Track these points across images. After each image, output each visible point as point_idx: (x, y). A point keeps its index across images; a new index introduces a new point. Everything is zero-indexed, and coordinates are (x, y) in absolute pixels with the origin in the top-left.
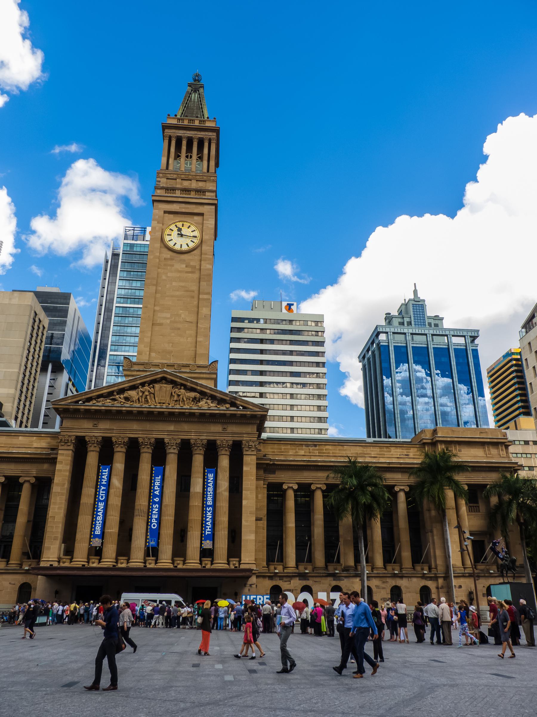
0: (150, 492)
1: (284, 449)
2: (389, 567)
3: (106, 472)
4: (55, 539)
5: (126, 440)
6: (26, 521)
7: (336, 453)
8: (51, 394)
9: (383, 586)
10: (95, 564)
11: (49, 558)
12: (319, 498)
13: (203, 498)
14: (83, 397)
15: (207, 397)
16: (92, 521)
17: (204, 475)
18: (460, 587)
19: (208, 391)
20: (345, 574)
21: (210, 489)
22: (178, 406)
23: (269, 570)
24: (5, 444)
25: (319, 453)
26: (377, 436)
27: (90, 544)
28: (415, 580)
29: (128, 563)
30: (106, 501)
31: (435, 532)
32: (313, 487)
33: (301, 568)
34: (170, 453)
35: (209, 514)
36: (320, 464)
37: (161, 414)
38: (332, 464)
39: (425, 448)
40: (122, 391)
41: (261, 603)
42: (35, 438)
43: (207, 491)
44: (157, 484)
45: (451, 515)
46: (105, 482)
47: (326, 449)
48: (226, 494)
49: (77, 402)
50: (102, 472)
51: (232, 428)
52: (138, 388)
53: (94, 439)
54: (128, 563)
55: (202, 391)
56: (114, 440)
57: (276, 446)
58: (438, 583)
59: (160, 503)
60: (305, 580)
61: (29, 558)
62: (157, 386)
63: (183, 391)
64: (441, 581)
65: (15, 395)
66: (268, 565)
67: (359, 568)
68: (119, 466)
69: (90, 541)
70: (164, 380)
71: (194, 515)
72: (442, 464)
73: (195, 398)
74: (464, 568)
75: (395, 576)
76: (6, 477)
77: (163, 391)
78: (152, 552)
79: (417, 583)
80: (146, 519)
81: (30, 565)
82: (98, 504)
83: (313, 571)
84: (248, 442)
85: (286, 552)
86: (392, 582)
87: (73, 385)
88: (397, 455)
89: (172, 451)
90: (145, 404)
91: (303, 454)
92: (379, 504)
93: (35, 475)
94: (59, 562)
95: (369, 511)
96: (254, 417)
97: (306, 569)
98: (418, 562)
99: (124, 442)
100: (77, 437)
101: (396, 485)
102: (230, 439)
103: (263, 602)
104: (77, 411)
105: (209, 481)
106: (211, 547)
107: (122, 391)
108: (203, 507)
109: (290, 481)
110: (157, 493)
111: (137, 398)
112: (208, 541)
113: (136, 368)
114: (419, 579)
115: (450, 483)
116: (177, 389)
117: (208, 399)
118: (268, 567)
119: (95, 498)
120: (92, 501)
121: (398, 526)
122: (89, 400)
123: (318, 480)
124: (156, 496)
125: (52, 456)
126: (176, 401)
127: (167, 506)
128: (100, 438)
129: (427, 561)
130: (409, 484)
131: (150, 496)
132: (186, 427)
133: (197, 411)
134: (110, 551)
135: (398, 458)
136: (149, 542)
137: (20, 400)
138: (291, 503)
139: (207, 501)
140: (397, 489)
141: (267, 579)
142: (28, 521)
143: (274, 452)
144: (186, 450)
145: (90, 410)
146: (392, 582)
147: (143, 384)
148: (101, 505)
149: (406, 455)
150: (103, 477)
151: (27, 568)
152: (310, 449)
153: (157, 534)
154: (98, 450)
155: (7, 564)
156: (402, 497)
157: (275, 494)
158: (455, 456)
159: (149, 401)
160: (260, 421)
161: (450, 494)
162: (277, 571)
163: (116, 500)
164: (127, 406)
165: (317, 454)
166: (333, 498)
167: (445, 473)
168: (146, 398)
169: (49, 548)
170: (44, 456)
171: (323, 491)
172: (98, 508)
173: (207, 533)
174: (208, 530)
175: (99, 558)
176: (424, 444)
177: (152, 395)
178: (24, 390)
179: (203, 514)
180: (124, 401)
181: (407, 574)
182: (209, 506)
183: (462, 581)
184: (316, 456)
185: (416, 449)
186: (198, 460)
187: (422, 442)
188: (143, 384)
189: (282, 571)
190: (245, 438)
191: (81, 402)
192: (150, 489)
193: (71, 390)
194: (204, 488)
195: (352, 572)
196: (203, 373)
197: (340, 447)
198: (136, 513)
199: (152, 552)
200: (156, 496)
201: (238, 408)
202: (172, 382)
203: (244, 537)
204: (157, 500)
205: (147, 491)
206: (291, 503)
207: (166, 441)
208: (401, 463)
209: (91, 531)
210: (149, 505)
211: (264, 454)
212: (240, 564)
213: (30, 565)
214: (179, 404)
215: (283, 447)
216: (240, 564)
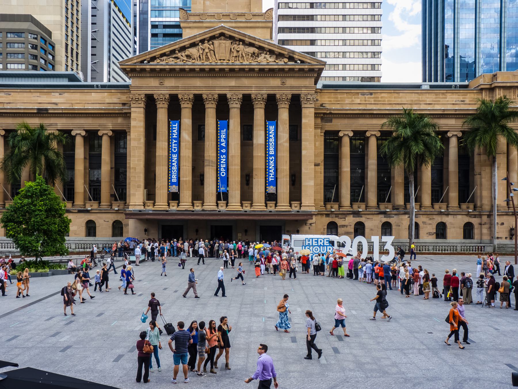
0: (217, 145)
1: (341, 98)
2: (437, 206)
3: (175, 127)
4: (139, 187)
5: (191, 96)
6: (109, 168)
7: (391, 101)
8: (95, 16)
9: (430, 222)
10: (174, 207)
11: (135, 203)
12: (373, 144)
13: (266, 148)
14: (148, 57)
15: (265, 52)
16: (169, 170)
17: (266, 128)
18: (503, 224)
19: (266, 46)
20: (395, 212)
21: (272, 140)
22: (237, 63)
23: (326, 209)
24: (80, 100)
25: (374, 101)
26: (433, 81)
27: (168, 191)
28: (459, 217)
29: (203, 206)
30: (179, 153)
31: (483, 173)
32: (368, 134)
33: (355, 207)
34: (233, 108)
35: (272, 162)
36: (375, 112)
37: (222, 70)
38: (387, 112)
39: (482, 93)
40: (183, 49)
41: (322, 245)
42: (106, 94)
43: (269, 142)
44: (223, 136)
45: (501, 160)
47: (381, 97)
48: (287, 145)
49: (142, 62)
50: (172, 127)
51: (291, 82)
52: (198, 45)
53: (162, 96)
54: (203, 206)
55: (260, 46)
56: (180, 97)
57: (332, 95)
58: (481, 220)
59: (227, 154)
60: (359, 217)
61: (116, 200)
62: (216, 42)
63: (241, 47)
64: (485, 218)
65: (61, 22)
66: (325, 204)
67: (408, 206)
68: (187, 120)
69: (168, 188)
70: (222, 35)
71: (258, 164)
72: (497, 114)
73: (254, 53)
74: (508, 207)
75: (441, 213)
76: (86, 131)
77: (222, 47)
78: (223, 196)
79: (462, 220)
80: (215, 168)
81: (119, 206)
82: (172, 156)
83: (366, 209)
84: (306, 95)
85: (341, 193)
86: (439, 219)
87: (115, 4)
88: (453, 101)
89: (235, 105)
90: (206, 61)
91: (359, 102)
92: (430, 153)
93: (111, 128)
94: (144, 205)
95: (421, 159)
96: (311, 70)
97: (359, 207)
98: (464, 202)
99: (190, 99)
100: (146, 95)
101: (449, 131)
102: (289, 93)
103: (323, 243)
104: (143, 70)
105: (270, 133)
106: (275, 192)
107: (183, 49)
108: (266, 157)
109: (346, 129)
110: (223, 145)
111: (198, 56)
112: (272, 187)
113: (192, 19)
114: (465, 216)
115: (503, 131)
116: (235, 45)
117: (266, 54)
118: (325, 207)
119: (169, 150)
120: (166, 154)
121: (448, 168)
122: (153, 59)
123: (373, 127)
125: (124, 111)
126: (236, 56)
127: (232, 156)
128: (167, 96)
129: (473, 201)
130: (463, 130)
131: (217, 148)
132: (246, 82)
133: (256, 67)
134: (186, 195)
135: (453, 104)
136: (220, 189)
137: (67, 27)
138: (346, 150)
139: (269, 151)
140: (449, 134)
141: (325, 215)
142: (111, 168)
143: (331, 101)
144: (247, 104)
145: (155, 69)
146: (439, 219)
147: (202, 41)
148: (175, 157)
149: (462, 101)
150: (174, 131)
151: (117, 209)
152: (365, 98)
153: (226, 181)
154: (166, 106)
155: (100, 205)
156: (453, 143)
157: (332, 141)
158: (512, 102)
159: (210, 58)
160: (318, 73)
161: (502, 140)
162: (333, 210)
163: (187, 152)
164: (189, 64)
165: (373, 102)
166: (386, 147)
167: (500, 121)
168: (207, 55)
169: (134, 195)
170: (117, 112)
171: (378, 139)
172: (172, 159)
173: (270, 179)
174: (272, 177)
175: (177, 202)
176: (482, 89)
177: (212, 52)
178: (70, 16)
179: (266, 163)
180: (185, 59)
181: (453, 212)
182: (271, 156)
183: (504, 219)
184: (371, 104)
185: (472, 95)
186: (259, 114)
187: (480, 88)
188: (202, 41)
189: (337, 209)
190: (303, 92)
191: (145, 62)
192: (217, 142)
193: (113, 10)
194: (266, 139)
195: (402, 211)
196: (259, 22)
197: (396, 95)
198: (206, 164)
199: (223, 196)
200: (222, 148)
201: (296, 62)
202: (231, 38)
203: (304, 183)
204: (224, 151)
205: (215, 143)
206: (346, 150)
207: (229, 96)
208: (456, 110)
209: (168, 179)
210: (217, 156)
211: (321, 103)
212: (301, 206)
213: (119, 206)
214: (239, 60)
215: (339, 96)
216: (301, 206)
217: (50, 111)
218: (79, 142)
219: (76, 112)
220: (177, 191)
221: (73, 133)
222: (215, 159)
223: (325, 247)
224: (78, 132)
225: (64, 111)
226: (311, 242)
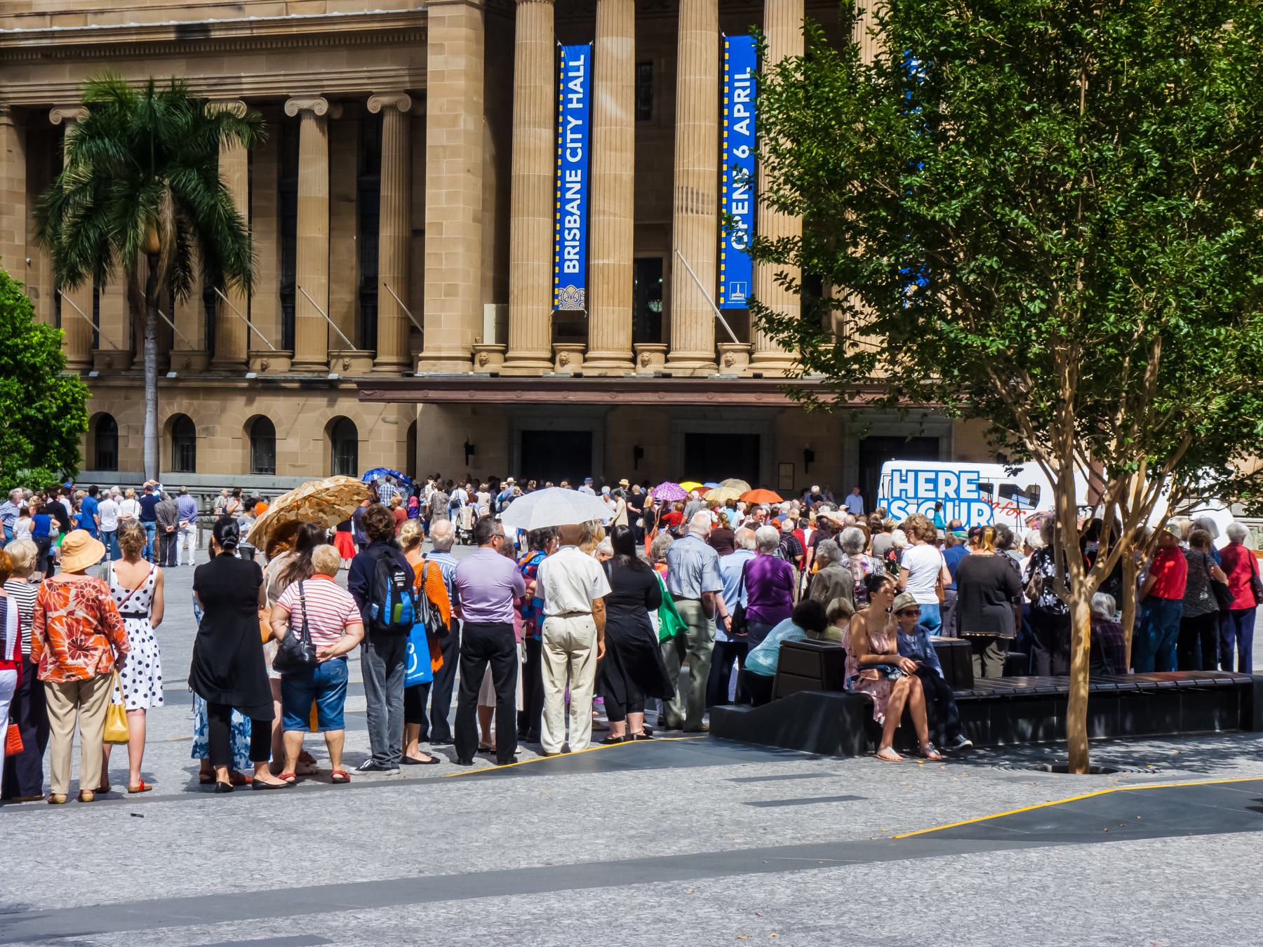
3: (577, 69)
11: (440, 349)
30: (587, 165)
46: (579, 101)
50: (567, 69)
69: (554, 297)
76: (333, 99)
82: (563, 177)
93: (408, 86)
103: (957, 491)
110: (742, 128)
124: (737, 140)
134: (612, 322)
148: (574, 180)
150: (571, 85)
163: (616, 162)
169: (437, 321)
192: (721, 117)
200: (737, 140)
210: (720, 173)
217: (215, 34)
218: (313, 141)
219: (294, 30)
220: (581, 308)
221: (291, 109)
222: (714, 182)
223: (964, 505)
224: (305, 104)
225: (256, 32)
226: (910, 486)
